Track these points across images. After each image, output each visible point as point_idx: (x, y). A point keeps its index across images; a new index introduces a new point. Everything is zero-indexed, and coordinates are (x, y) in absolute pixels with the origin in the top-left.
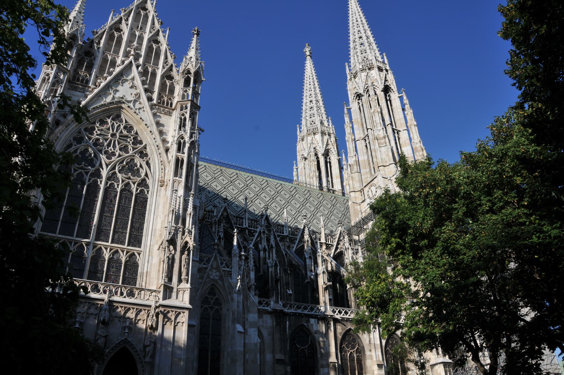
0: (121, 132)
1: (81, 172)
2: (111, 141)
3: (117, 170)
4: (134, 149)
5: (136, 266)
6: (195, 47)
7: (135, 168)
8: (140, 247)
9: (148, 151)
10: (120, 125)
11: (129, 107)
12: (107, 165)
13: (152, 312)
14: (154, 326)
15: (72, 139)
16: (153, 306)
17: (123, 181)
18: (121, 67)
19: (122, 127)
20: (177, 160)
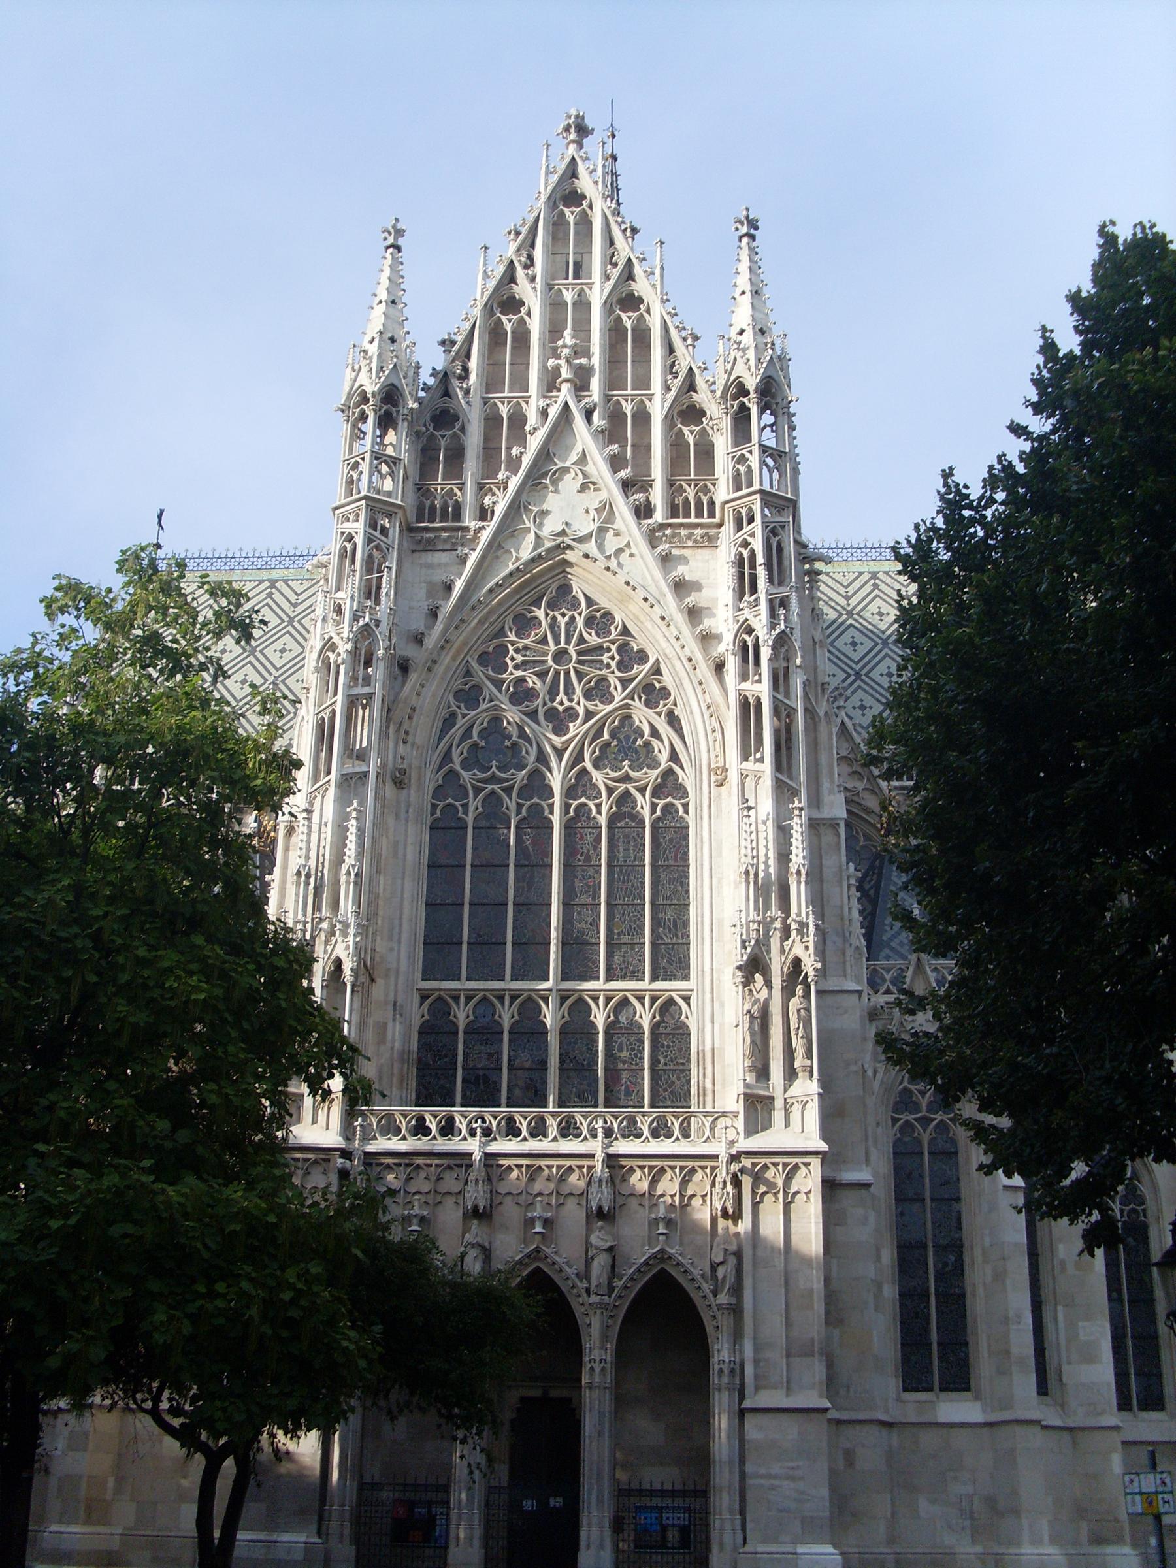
1: (493, 792)
2: (557, 673)
3: (588, 765)
4: (625, 683)
5: (682, 1033)
6: (748, 288)
7: (639, 742)
8: (686, 977)
9: (667, 680)
10: (573, 618)
11: (587, 556)
12: (560, 753)
13: (722, 1174)
14: (731, 1211)
15: (451, 698)
16: (724, 1157)
17: (610, 791)
18: (542, 434)
19: (580, 622)
20: (744, 704)
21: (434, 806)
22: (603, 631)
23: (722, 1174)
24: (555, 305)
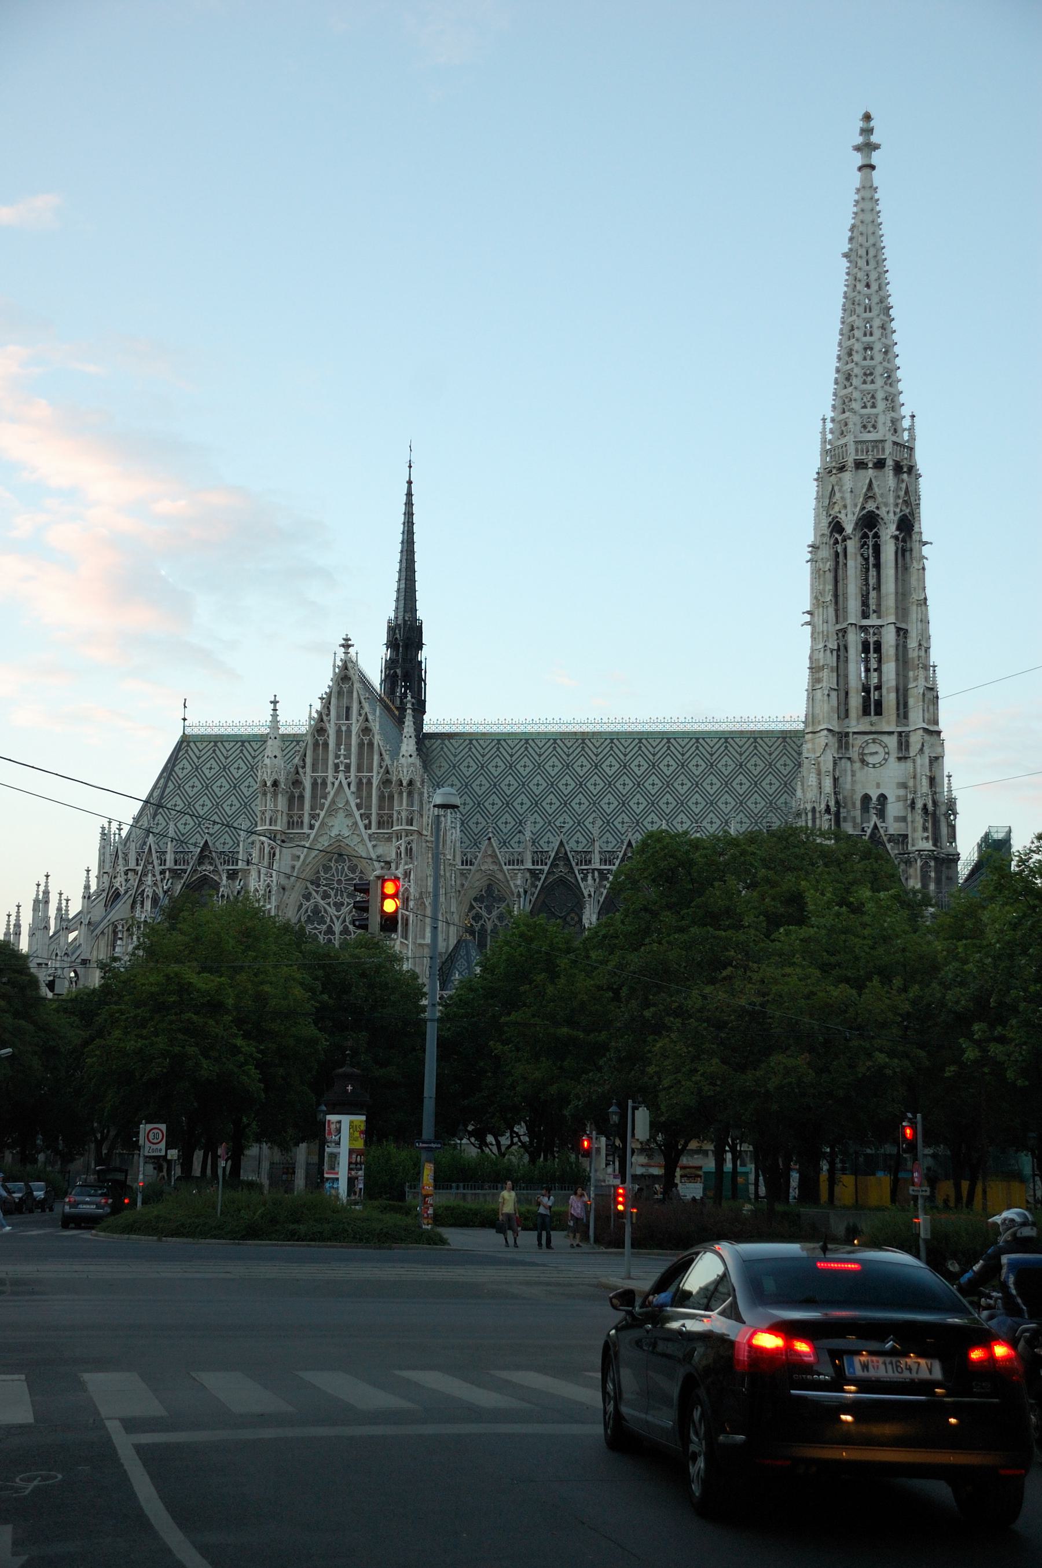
0: (346, 875)
12: (338, 918)
18: (332, 793)
22: (354, 872)
24: (339, 732)
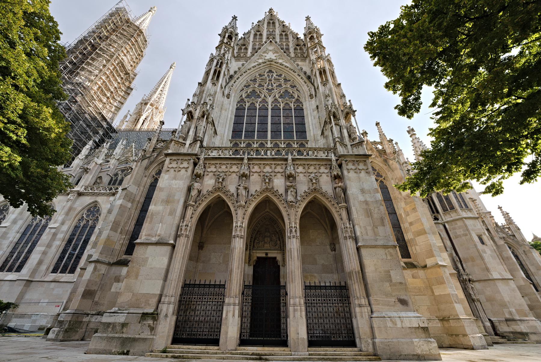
13: (334, 163)
21: (237, 105)
23: (334, 163)
